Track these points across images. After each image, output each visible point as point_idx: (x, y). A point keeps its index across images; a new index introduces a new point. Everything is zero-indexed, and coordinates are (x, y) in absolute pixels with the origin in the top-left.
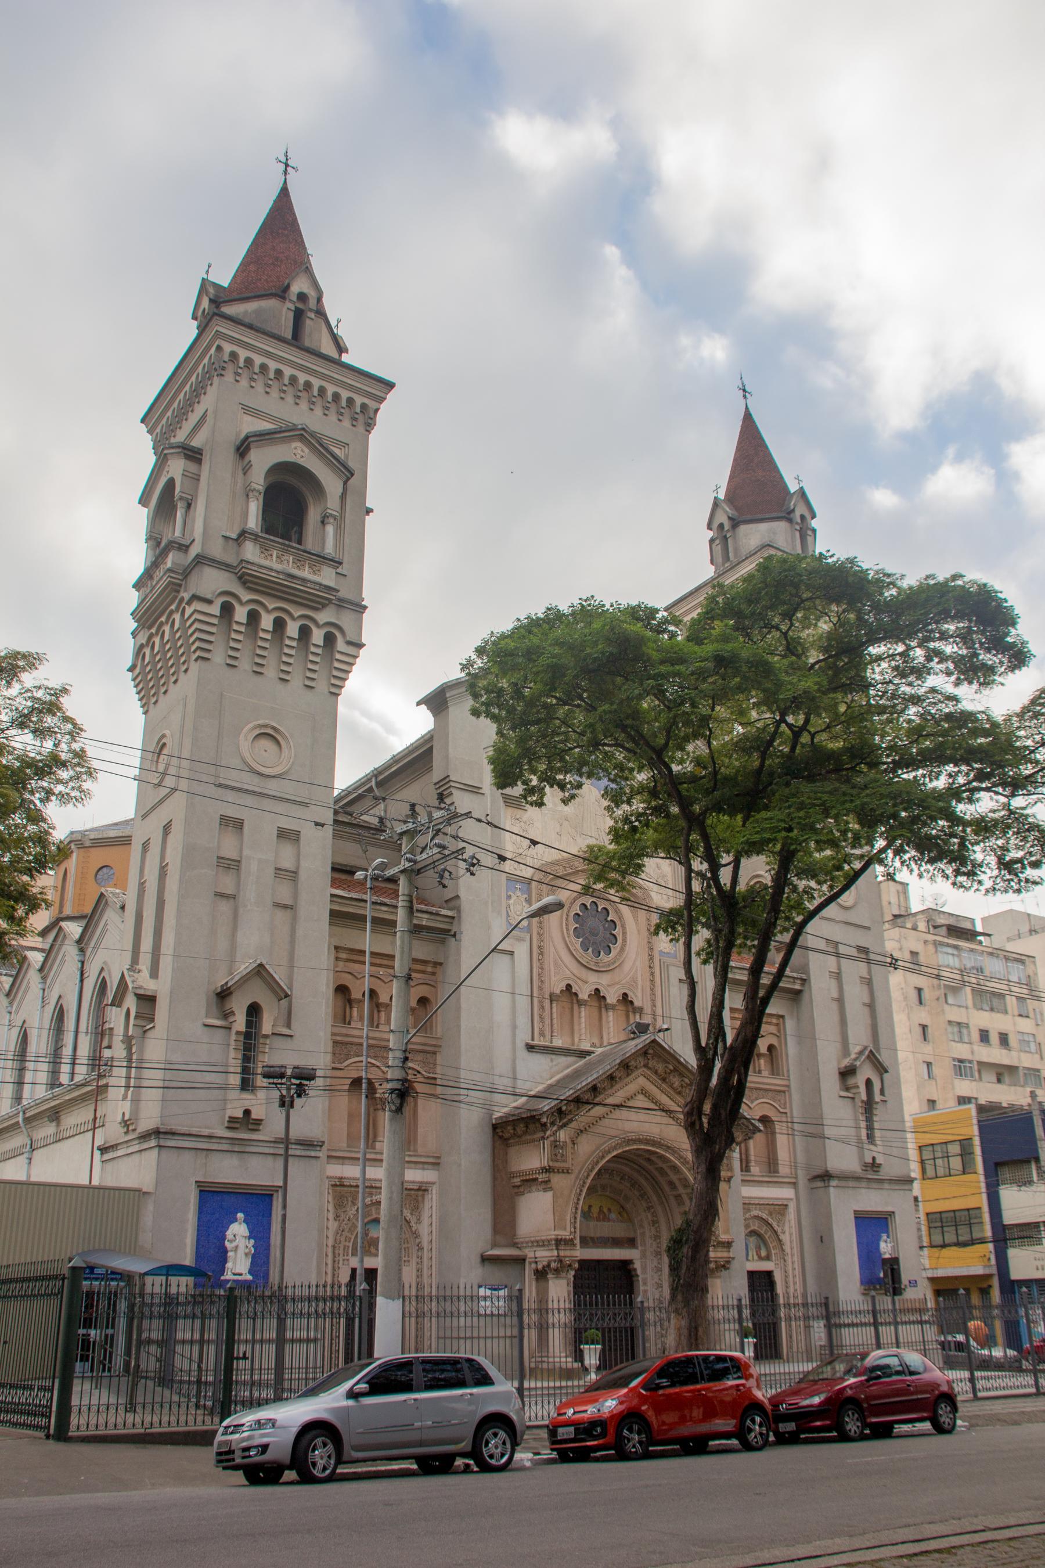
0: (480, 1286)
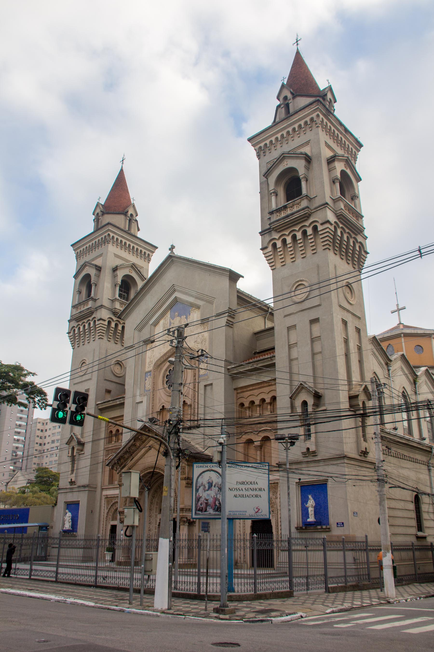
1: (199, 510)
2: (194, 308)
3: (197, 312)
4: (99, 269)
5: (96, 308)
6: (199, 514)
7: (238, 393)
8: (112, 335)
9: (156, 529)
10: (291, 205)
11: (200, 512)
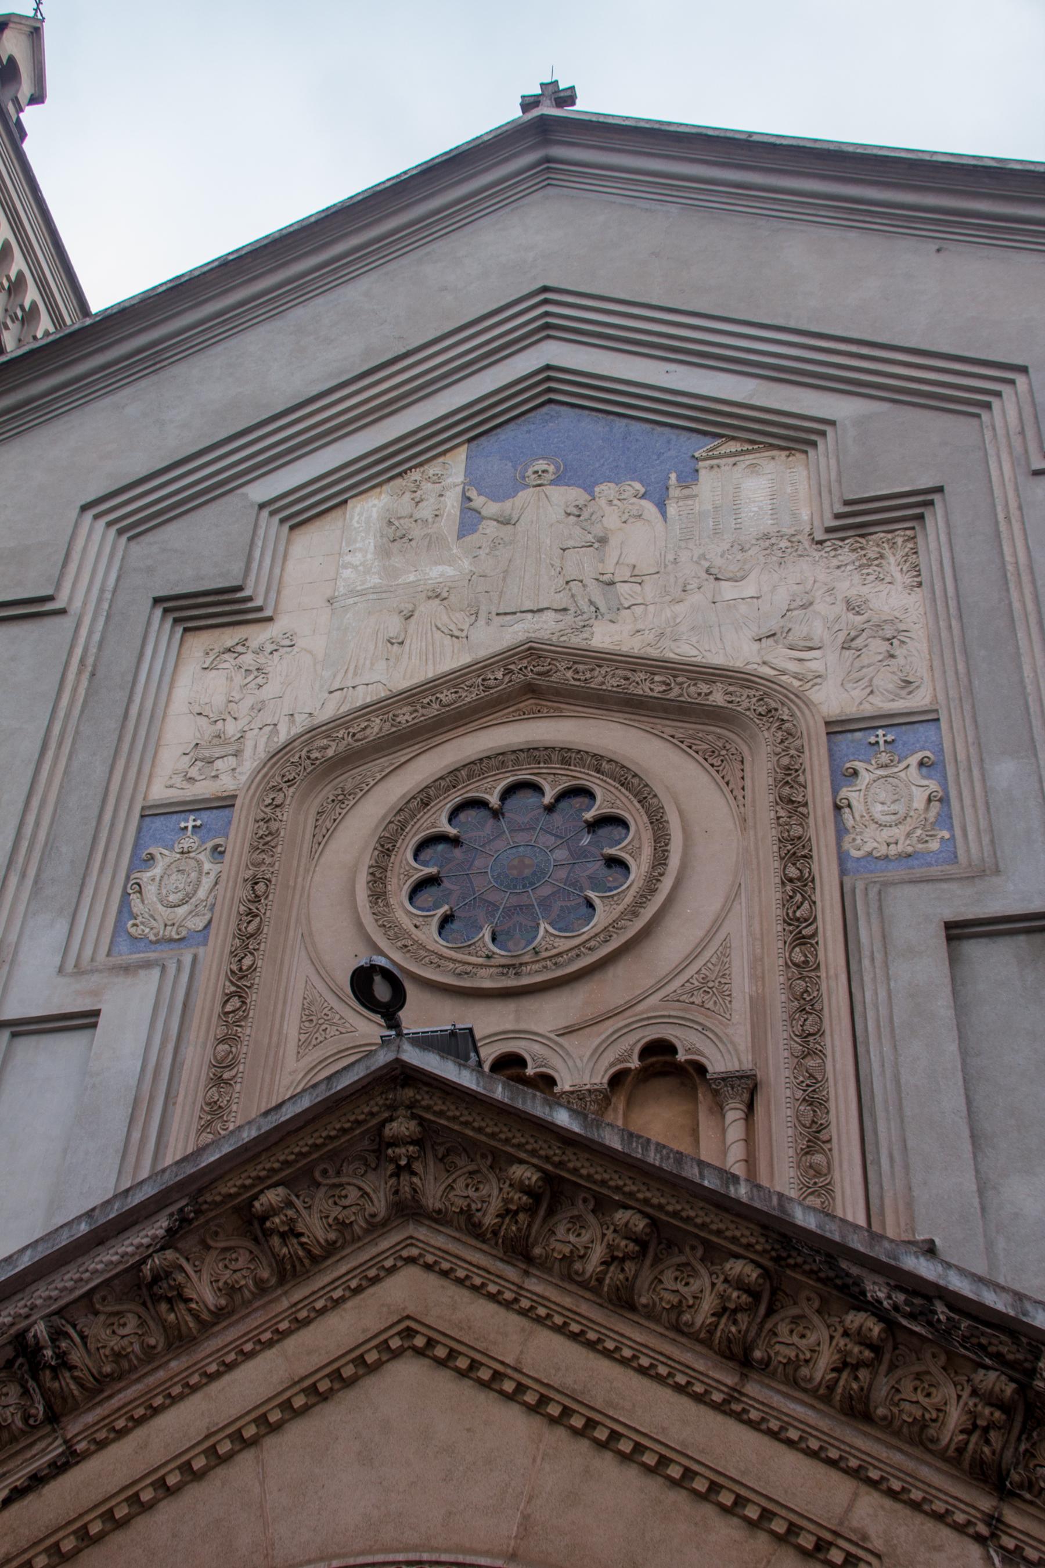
2: (733, 447)
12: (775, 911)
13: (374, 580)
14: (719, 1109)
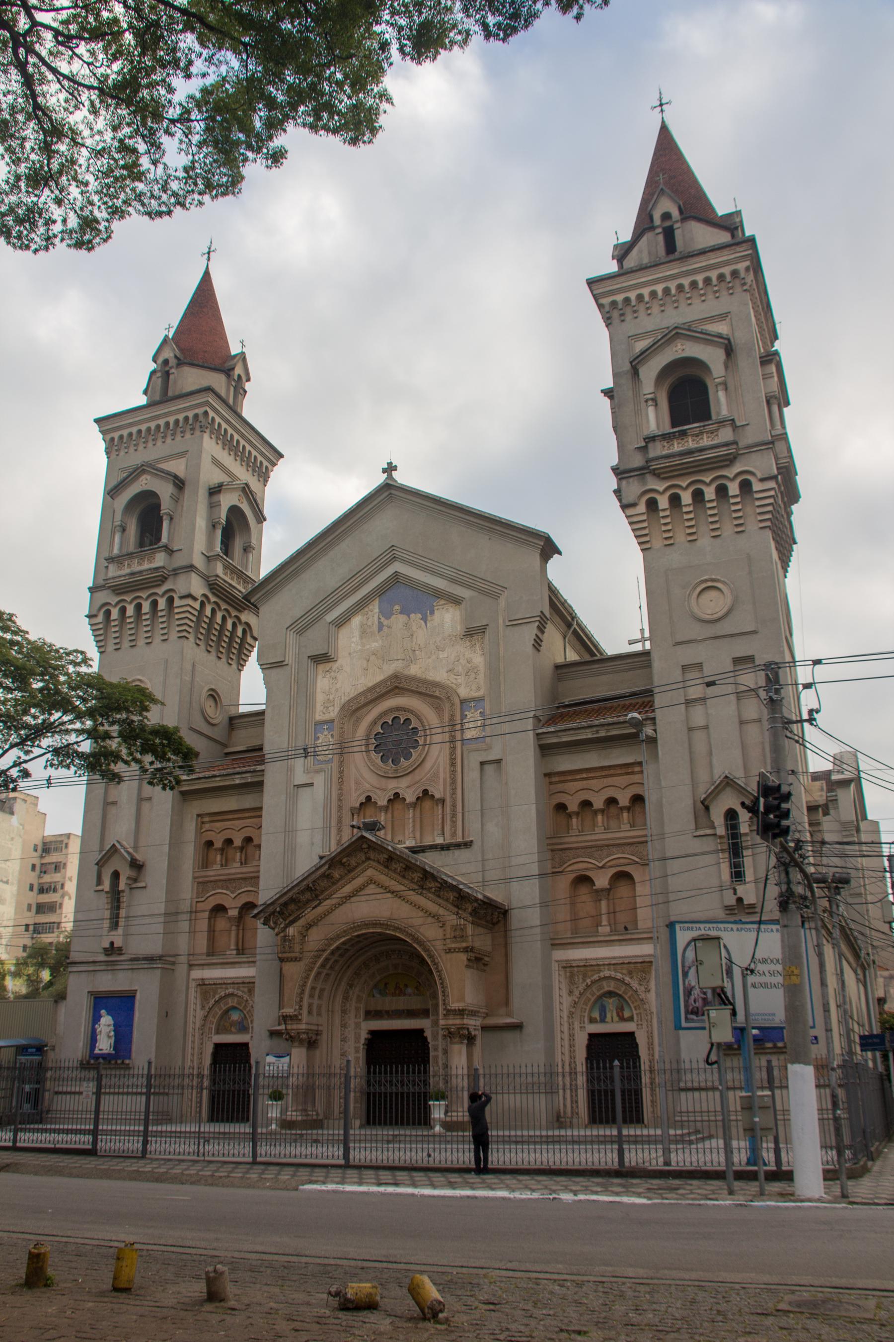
0: (268, 1055)
1: (692, 1013)
2: (443, 602)
3: (451, 610)
4: (179, 484)
5: (174, 570)
6: (693, 1021)
7: (551, 783)
8: (203, 631)
9: (357, 1051)
10: (697, 431)
11: (694, 1017)
12: (448, 757)
13: (360, 647)
14: (437, 805)
